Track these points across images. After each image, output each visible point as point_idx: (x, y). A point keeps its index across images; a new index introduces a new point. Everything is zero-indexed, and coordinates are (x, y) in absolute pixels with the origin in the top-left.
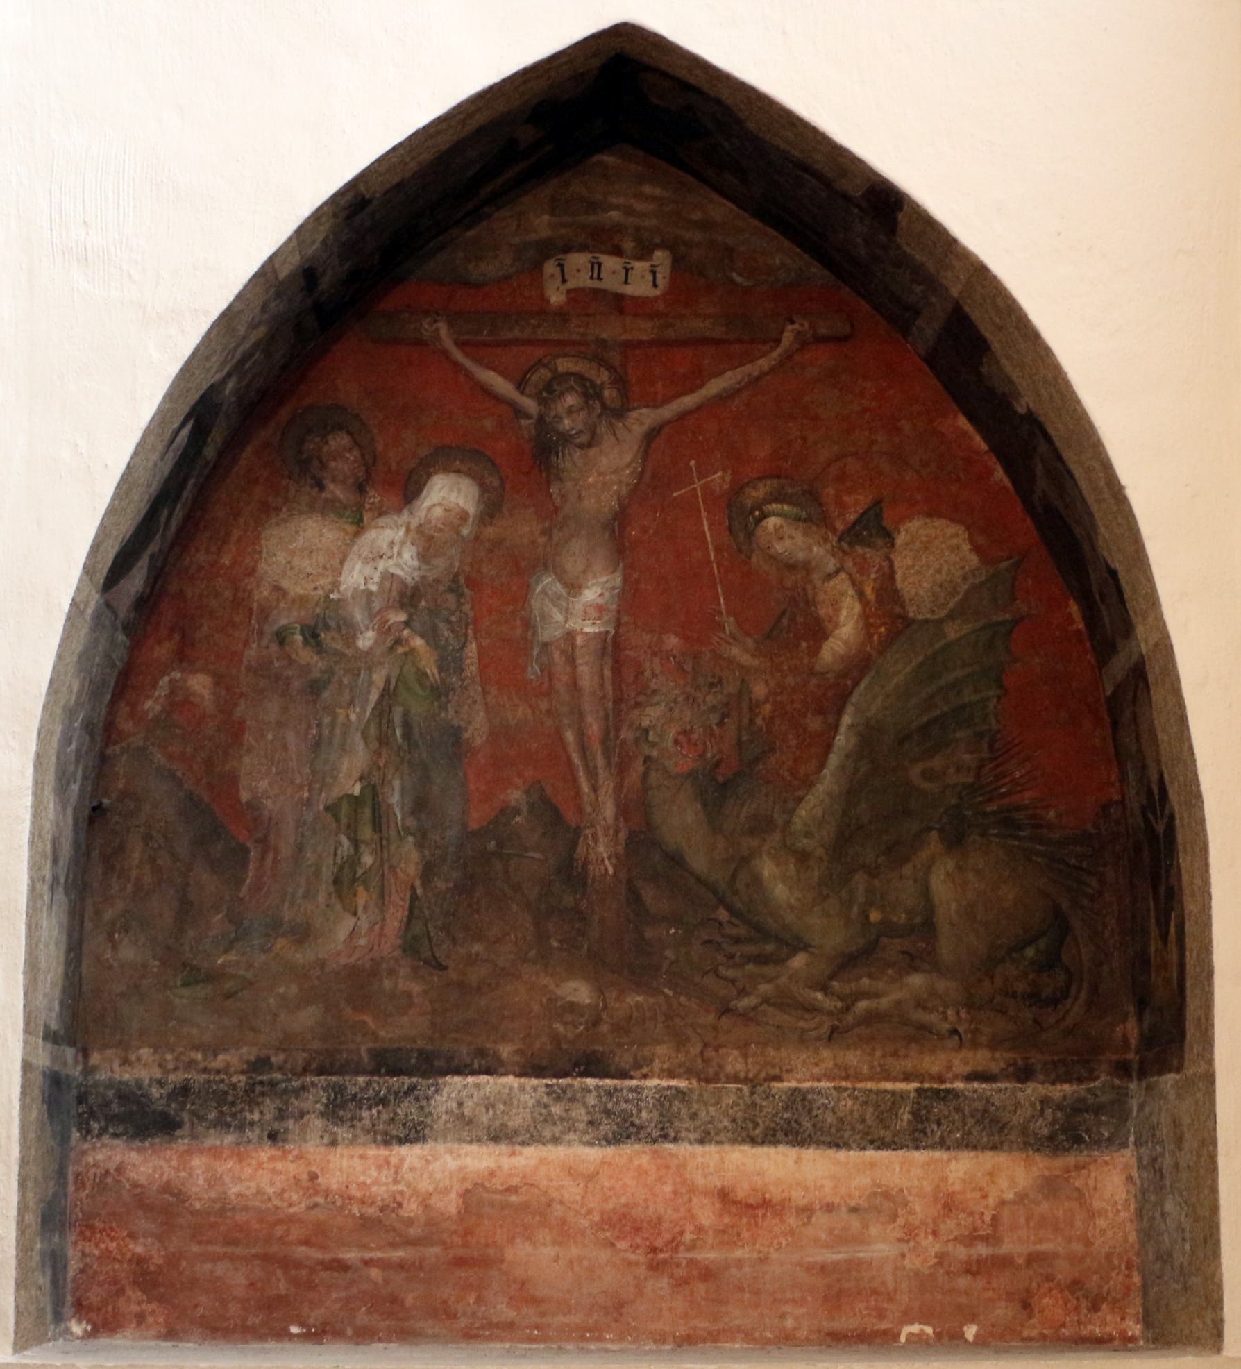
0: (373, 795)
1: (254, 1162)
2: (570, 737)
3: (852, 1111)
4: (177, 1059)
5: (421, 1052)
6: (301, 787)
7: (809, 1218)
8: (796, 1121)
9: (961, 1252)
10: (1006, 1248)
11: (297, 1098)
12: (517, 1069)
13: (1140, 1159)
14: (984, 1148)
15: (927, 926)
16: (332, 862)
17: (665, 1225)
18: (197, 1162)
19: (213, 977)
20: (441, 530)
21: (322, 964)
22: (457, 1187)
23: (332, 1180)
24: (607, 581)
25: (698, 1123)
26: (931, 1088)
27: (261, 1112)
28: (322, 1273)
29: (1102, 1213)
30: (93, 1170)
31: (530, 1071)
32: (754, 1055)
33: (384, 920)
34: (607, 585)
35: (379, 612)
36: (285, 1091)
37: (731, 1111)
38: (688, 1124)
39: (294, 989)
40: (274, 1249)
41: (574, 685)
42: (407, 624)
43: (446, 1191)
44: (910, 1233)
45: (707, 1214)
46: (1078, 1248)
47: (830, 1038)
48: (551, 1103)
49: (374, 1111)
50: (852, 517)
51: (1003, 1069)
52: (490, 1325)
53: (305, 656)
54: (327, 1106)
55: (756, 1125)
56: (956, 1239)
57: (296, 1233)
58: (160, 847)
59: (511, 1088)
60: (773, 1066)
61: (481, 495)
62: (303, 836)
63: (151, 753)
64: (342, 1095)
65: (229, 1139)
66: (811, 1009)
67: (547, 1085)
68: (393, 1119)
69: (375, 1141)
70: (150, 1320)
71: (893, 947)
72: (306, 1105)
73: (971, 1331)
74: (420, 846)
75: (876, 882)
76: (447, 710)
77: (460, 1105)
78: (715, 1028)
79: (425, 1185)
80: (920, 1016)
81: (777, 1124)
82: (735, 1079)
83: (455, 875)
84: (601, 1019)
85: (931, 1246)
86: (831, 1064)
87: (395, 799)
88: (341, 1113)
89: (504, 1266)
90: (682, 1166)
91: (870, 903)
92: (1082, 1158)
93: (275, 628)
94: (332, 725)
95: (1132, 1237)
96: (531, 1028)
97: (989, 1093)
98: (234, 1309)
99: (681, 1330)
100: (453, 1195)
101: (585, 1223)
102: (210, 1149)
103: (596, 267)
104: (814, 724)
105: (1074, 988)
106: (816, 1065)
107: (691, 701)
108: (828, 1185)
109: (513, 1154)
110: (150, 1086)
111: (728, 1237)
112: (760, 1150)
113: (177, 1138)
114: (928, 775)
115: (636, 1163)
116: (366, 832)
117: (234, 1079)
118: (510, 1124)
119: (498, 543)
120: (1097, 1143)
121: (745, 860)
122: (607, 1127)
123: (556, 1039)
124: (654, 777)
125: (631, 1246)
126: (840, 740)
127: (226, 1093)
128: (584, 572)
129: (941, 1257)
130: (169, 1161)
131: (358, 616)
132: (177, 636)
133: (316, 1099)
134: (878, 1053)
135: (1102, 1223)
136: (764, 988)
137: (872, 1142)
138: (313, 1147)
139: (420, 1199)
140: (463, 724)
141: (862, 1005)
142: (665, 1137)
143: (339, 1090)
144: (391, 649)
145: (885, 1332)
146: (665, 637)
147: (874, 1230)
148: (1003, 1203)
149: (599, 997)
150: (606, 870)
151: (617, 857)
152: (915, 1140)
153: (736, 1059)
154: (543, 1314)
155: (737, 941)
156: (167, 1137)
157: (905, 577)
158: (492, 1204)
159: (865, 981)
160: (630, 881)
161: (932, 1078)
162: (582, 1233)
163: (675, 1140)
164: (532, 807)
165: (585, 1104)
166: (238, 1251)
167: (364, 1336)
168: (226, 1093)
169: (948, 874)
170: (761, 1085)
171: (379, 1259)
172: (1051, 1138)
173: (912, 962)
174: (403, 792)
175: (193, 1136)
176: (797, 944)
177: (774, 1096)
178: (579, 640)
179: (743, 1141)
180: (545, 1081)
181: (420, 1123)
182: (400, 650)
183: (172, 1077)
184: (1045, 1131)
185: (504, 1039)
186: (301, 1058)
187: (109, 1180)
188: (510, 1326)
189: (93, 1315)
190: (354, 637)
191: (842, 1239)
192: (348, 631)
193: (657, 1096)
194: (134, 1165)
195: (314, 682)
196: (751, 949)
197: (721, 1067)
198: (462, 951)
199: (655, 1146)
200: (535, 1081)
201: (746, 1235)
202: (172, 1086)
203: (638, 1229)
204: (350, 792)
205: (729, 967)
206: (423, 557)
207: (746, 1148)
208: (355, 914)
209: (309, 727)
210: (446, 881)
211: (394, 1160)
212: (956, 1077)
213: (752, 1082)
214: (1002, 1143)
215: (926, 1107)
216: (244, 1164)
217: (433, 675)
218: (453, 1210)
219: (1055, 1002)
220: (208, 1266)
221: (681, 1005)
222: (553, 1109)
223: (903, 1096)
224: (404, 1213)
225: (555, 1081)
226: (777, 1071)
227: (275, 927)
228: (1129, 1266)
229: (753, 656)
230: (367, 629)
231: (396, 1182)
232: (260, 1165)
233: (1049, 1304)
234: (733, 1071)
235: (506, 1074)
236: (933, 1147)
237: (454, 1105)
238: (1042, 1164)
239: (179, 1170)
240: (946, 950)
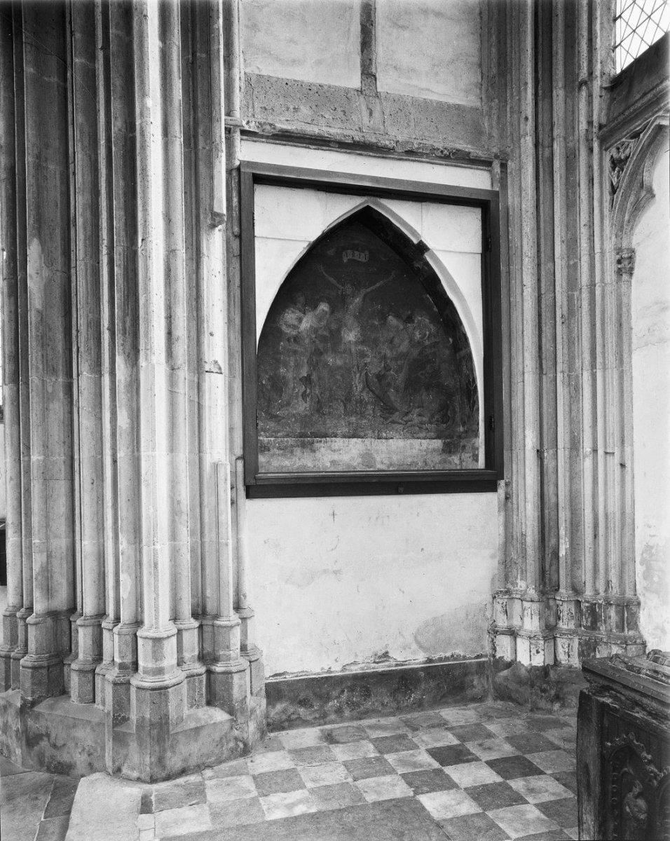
114: (422, 374)
176: (397, 410)
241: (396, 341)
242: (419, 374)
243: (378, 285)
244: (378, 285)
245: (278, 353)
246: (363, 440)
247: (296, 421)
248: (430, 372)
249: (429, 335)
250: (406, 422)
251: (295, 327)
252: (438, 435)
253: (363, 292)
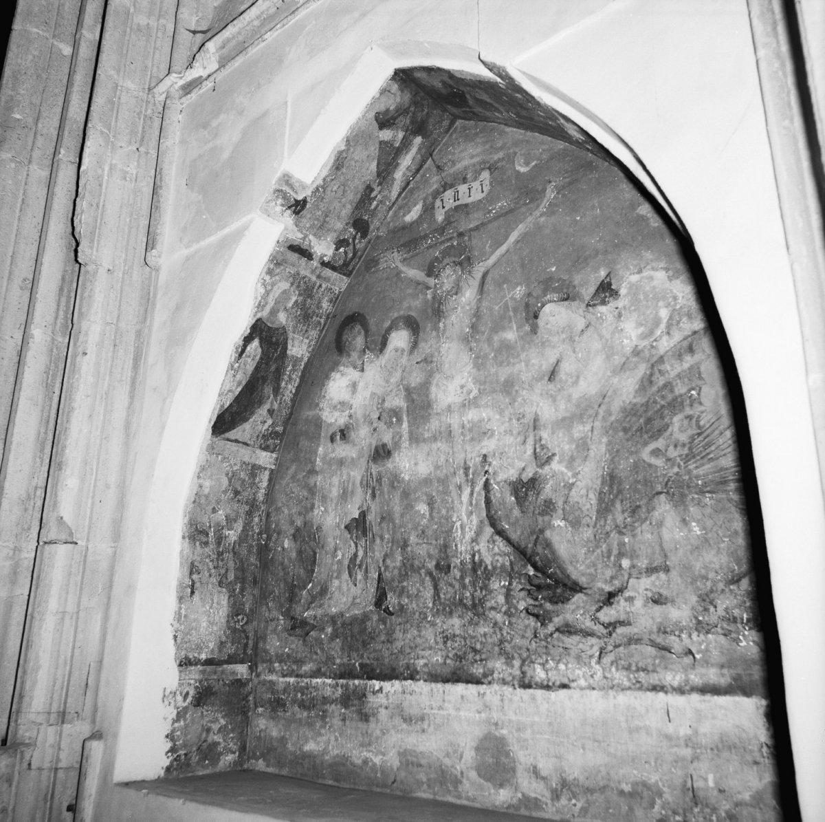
91: (621, 555)
114: (656, 453)
141: (620, 630)
241: (566, 367)
242: (645, 454)
245: (313, 472)
246: (482, 688)
247: (335, 636)
248: (683, 438)
249: (671, 318)
250: (612, 626)
251: (343, 405)
252: (737, 678)
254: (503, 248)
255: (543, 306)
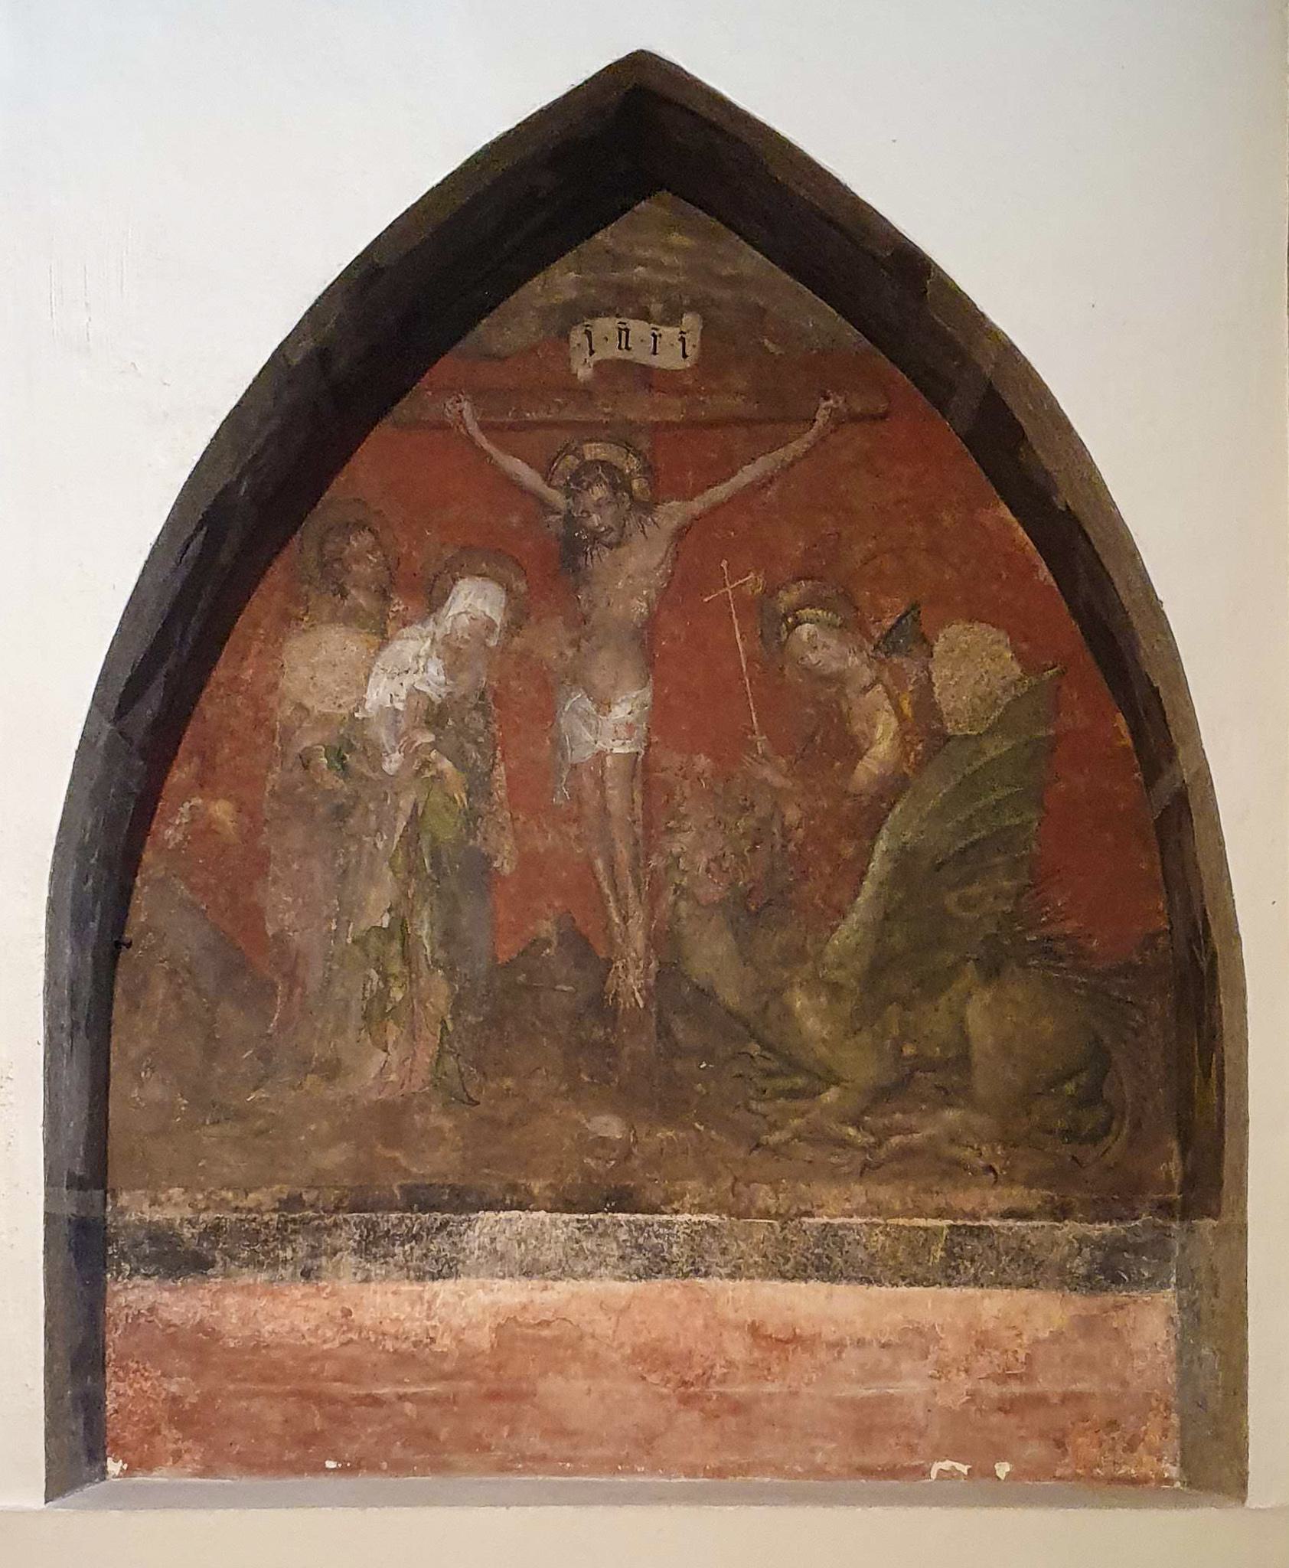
0: (400, 930)
1: (287, 1300)
2: (599, 864)
3: (883, 1247)
4: (208, 1198)
5: (452, 1187)
6: (329, 918)
7: (840, 1353)
8: (827, 1257)
9: (994, 1390)
10: (1041, 1386)
11: (329, 1235)
12: (549, 1206)
13: (1180, 1301)
14: (1018, 1287)
15: (963, 1062)
16: (361, 997)
17: (696, 1359)
18: (231, 1300)
19: (240, 1116)
20: (467, 642)
21: (352, 1100)
22: (490, 1323)
23: (365, 1317)
24: (637, 697)
25: (728, 1258)
26: (964, 1225)
27: (294, 1250)
28: (356, 1408)
29: (1141, 1353)
30: (126, 1311)
31: (560, 1205)
32: (785, 1190)
33: (415, 1054)
34: (637, 702)
35: (405, 733)
36: (318, 1228)
37: (761, 1246)
38: (719, 1259)
39: (325, 1125)
40: (309, 1385)
41: (604, 810)
42: (434, 745)
43: (478, 1326)
44: (942, 1370)
45: (737, 1348)
46: (1114, 1388)
47: (862, 1173)
48: (583, 1238)
49: (407, 1247)
50: (888, 623)
51: (1039, 1206)
52: (523, 1458)
53: (332, 781)
54: (359, 1242)
55: (788, 1260)
56: (987, 1378)
57: (330, 1368)
58: (185, 983)
59: (543, 1223)
60: (804, 1201)
61: (508, 603)
62: (330, 969)
63: (174, 885)
64: (375, 1232)
65: (263, 1277)
66: (844, 1143)
67: (578, 1221)
68: (425, 1255)
69: (408, 1278)
70: (187, 1457)
71: (927, 1080)
72: (338, 1243)
73: (1003, 1469)
74: (450, 979)
75: (911, 1016)
76: (475, 838)
77: (493, 1240)
78: (745, 1163)
79: (458, 1321)
80: (956, 1151)
81: (808, 1259)
82: (766, 1214)
83: (486, 1008)
84: (632, 1153)
85: (963, 1383)
86: (863, 1200)
87: (425, 931)
88: (374, 1250)
89: (536, 1400)
90: (713, 1300)
91: (904, 1037)
92: (1122, 1297)
93: (299, 750)
94: (359, 853)
95: (1172, 1379)
96: (562, 1162)
97: (1024, 1232)
98: (270, 1445)
99: (713, 1463)
100: (486, 1329)
101: (615, 1357)
102: (243, 1288)
103: (624, 333)
104: (849, 850)
105: (1115, 1126)
106: (847, 1200)
107: (722, 827)
108: (859, 1321)
109: (545, 1289)
110: (181, 1225)
111: (759, 1371)
112: (789, 1284)
113: (209, 1277)
114: (965, 903)
115: (667, 1297)
116: (396, 967)
117: (266, 1218)
118: (541, 1258)
119: (525, 655)
120: (1137, 1284)
121: (778, 992)
122: (638, 1262)
123: (587, 1173)
124: (683, 905)
125: (662, 1380)
126: (875, 866)
127: (258, 1232)
128: (614, 687)
129: (973, 1395)
130: (201, 1300)
131: (384, 736)
132: (196, 760)
133: (347, 1237)
134: (911, 1188)
135: (1139, 1364)
136: (796, 1122)
137: (903, 1278)
138: (347, 1284)
139: (453, 1333)
140: (492, 852)
141: (895, 1140)
142: (697, 1271)
143: (372, 1227)
144: (418, 773)
145: (916, 1468)
146: (696, 759)
147: (905, 1366)
148: (1037, 1341)
149: (630, 1131)
150: (637, 1004)
151: (648, 989)
152: (947, 1277)
153: (767, 1193)
154: (575, 1447)
155: (770, 1075)
156: (200, 1277)
157: (944, 688)
158: (525, 1338)
159: (898, 1116)
160: (659, 1013)
161: (966, 1215)
162: (613, 1366)
163: (706, 1275)
164: (562, 936)
165: (616, 1238)
166: (273, 1388)
167: (399, 1467)
168: (258, 1232)
169: (988, 1008)
170: (792, 1220)
171: (415, 1394)
172: (1088, 1277)
173: (947, 1097)
174: (432, 925)
175: (227, 1276)
176: (830, 1078)
177: (805, 1231)
178: (609, 762)
179: (774, 1276)
180: (576, 1216)
181: (452, 1259)
182: (428, 774)
183: (203, 1216)
184: (1082, 1271)
185: (536, 1175)
186: (333, 1195)
187: (142, 1320)
188: (543, 1458)
189: (129, 1454)
190: (381, 761)
191: (872, 1374)
192: (374, 754)
193: (688, 1231)
194: (167, 1306)
195: (339, 807)
196: (781, 1083)
197: (752, 1202)
198: (493, 1085)
199: (686, 1281)
200: (566, 1217)
201: (776, 1369)
202: (204, 1225)
203: (668, 1364)
204: (379, 925)
205: (759, 1100)
206: (450, 671)
207: (778, 1283)
208: (385, 1051)
209: (335, 855)
210: (477, 1015)
211: (427, 1296)
212: (990, 1214)
213: (784, 1218)
214: (1037, 1282)
215: (959, 1243)
216: (277, 1302)
217: (462, 801)
218: (486, 1345)
219: (1094, 1139)
220: (244, 1404)
221: (712, 1140)
222: (584, 1244)
223: (936, 1232)
224: (437, 1348)
225: (586, 1216)
226: (808, 1207)
227: (304, 1065)
228: (1167, 1408)
229: (785, 776)
230: (394, 752)
231: (429, 1318)
232: (294, 1303)
233: (1084, 1445)
234: (763, 1207)
235: (538, 1210)
236: (965, 1284)
237: (487, 1240)
238: (1080, 1303)
239: (212, 1309)
240: (981, 1088)
242: (951, 899)
243: (747, 474)
244: (747, 474)
253: (673, 513)
254: (720, 492)
255: (798, 623)
